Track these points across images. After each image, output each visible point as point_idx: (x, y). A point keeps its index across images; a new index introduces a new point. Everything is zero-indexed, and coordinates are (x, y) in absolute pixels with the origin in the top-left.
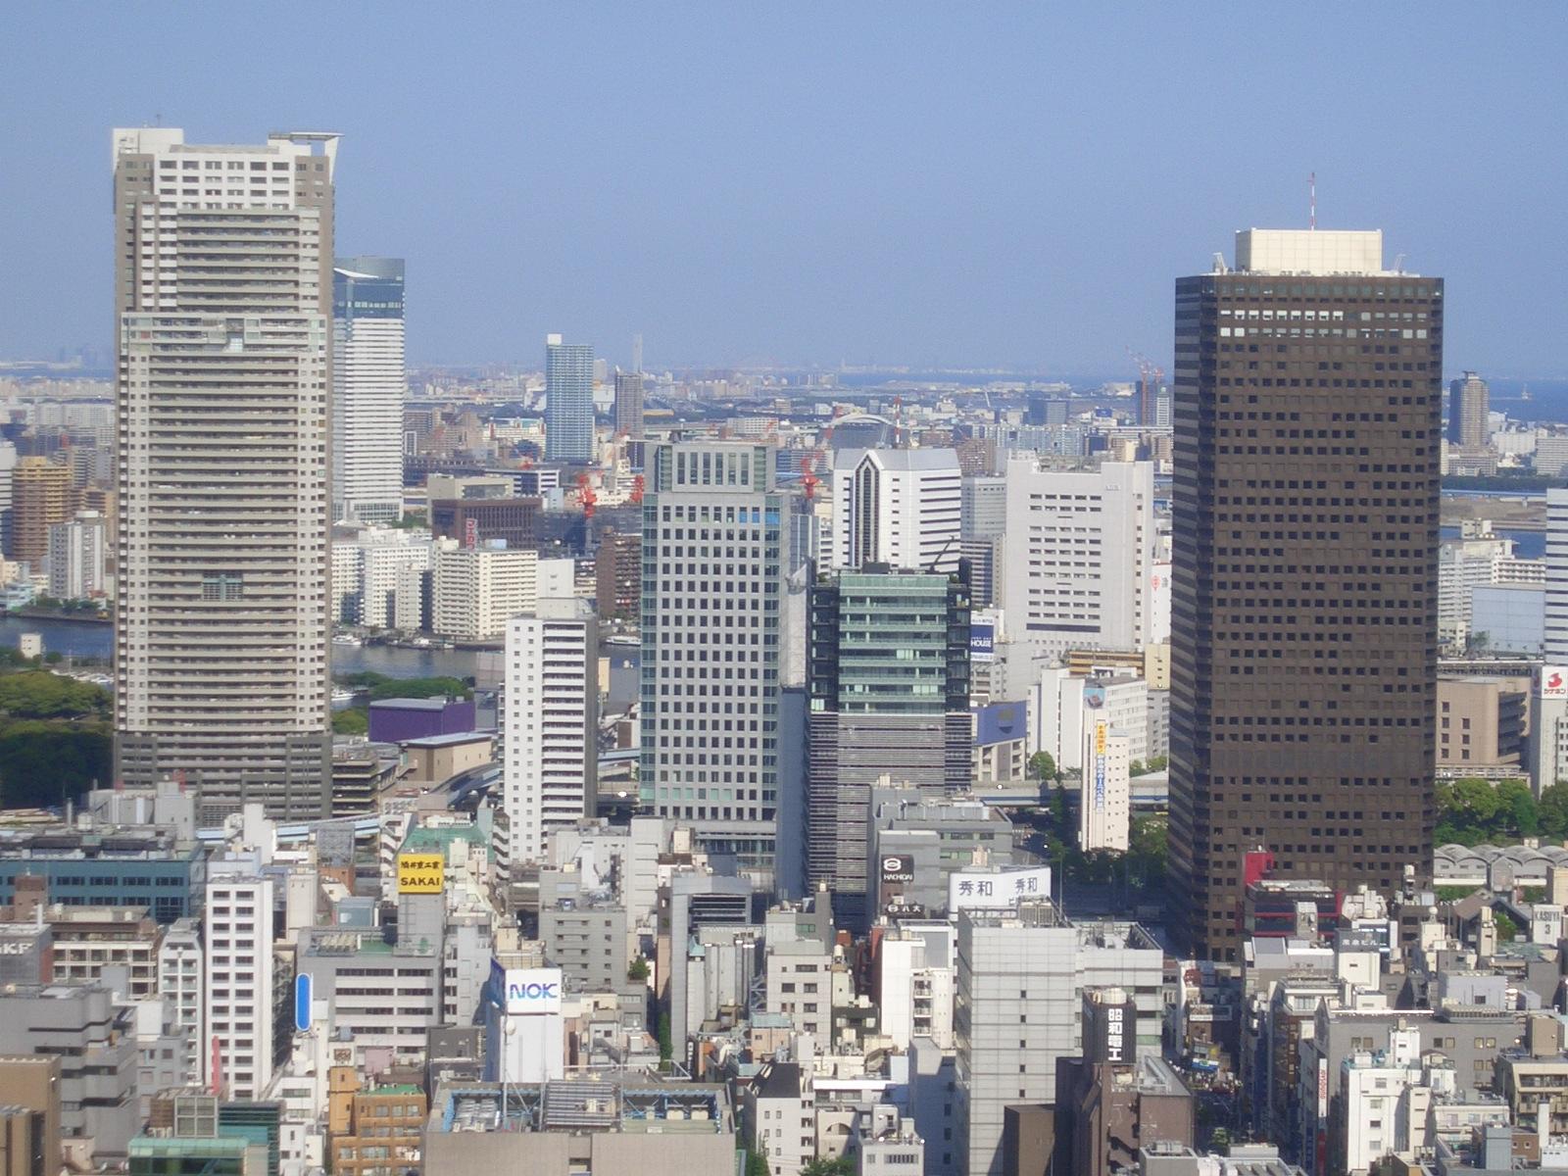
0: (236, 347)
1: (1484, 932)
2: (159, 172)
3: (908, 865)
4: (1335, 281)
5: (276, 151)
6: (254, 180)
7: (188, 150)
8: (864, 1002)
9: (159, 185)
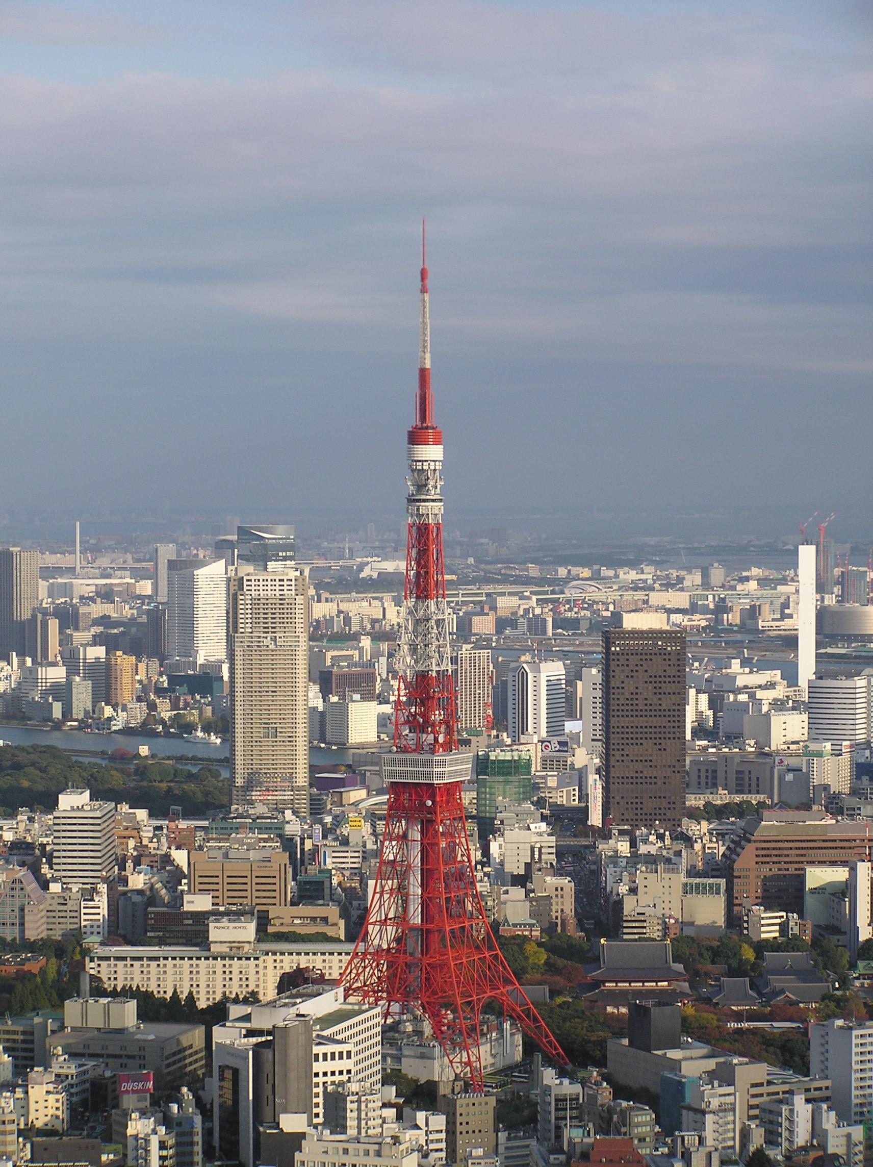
1: (666, 838)
2: (245, 583)
3: (502, 823)
4: (651, 631)
5: (287, 574)
6: (280, 585)
7: (256, 575)
8: (485, 859)
9: (245, 588)
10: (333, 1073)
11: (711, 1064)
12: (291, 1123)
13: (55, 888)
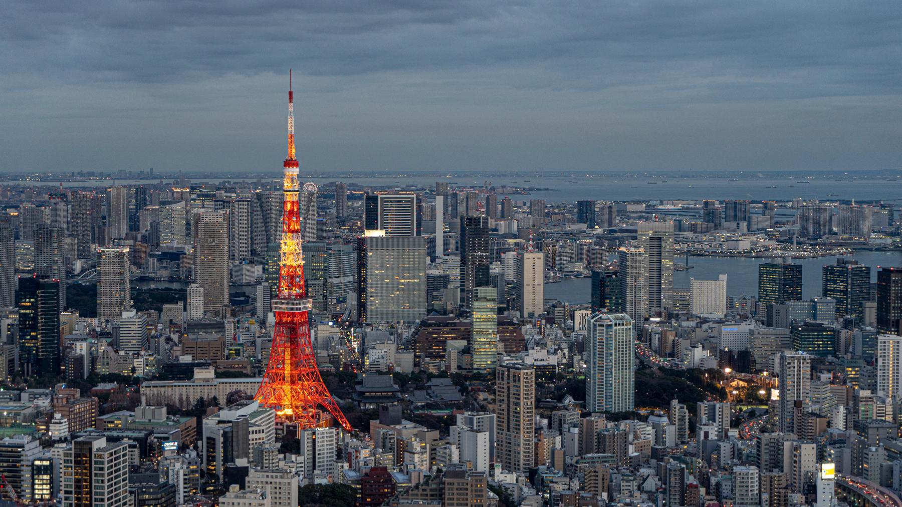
0: (213, 244)
3: (315, 321)
10: (256, 439)
11: (416, 431)
12: (241, 462)
13: (122, 353)
